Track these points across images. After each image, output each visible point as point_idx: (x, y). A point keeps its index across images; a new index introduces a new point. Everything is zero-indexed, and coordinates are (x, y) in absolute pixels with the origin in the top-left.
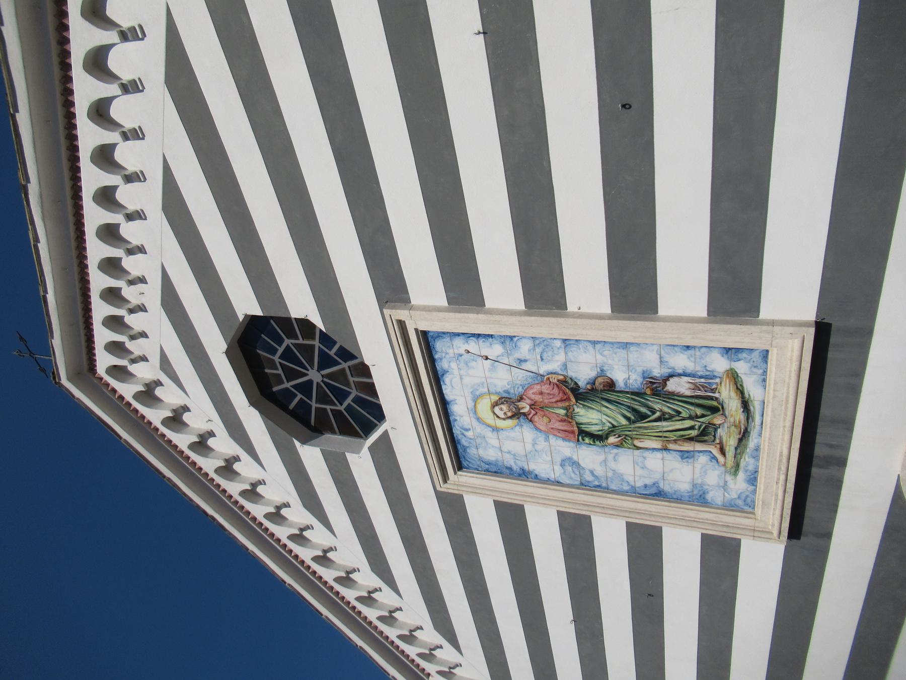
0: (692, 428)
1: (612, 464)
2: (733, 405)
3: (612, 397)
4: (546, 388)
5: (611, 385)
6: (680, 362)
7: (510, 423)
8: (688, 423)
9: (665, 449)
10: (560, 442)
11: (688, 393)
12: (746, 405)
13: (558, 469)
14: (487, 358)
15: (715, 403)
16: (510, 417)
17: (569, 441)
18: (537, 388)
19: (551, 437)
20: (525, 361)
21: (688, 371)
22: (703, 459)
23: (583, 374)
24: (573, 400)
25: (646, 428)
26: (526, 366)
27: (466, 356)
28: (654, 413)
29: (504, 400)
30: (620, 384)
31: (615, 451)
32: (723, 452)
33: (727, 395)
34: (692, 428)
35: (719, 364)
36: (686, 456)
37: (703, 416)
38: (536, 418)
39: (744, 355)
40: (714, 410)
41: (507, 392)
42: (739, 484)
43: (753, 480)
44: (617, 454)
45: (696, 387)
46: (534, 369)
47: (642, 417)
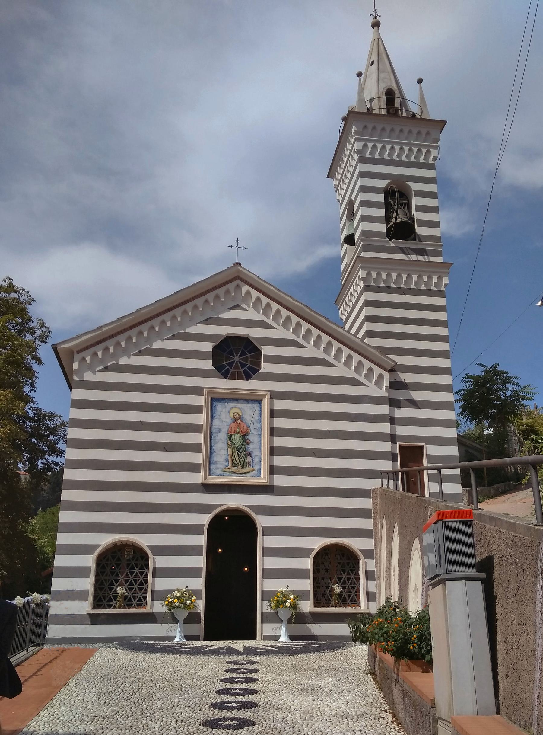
0: (236, 461)
1: (220, 442)
2: (244, 470)
3: (244, 444)
4: (245, 428)
5: (248, 444)
6: (256, 460)
7: (233, 417)
8: (238, 461)
9: (228, 455)
10: (227, 429)
11: (247, 461)
12: (245, 473)
13: (217, 427)
14: (254, 415)
15: (245, 467)
16: (234, 417)
17: (228, 431)
18: (245, 426)
19: (229, 427)
20: (254, 424)
21: (254, 461)
22: (226, 464)
23: (251, 438)
24: (242, 434)
25: (235, 451)
26: (252, 425)
27: (254, 410)
28: (240, 453)
29: (240, 417)
30: (248, 446)
31: (226, 443)
32: (229, 468)
33: (247, 469)
34: (236, 461)
35: (256, 468)
36: (227, 460)
37: (241, 464)
38: (234, 424)
39: (259, 472)
40: (243, 466)
41: (243, 418)
42: (218, 472)
43: (220, 475)
44: (224, 443)
45: (249, 463)
46: (251, 426)
47: (239, 450)
